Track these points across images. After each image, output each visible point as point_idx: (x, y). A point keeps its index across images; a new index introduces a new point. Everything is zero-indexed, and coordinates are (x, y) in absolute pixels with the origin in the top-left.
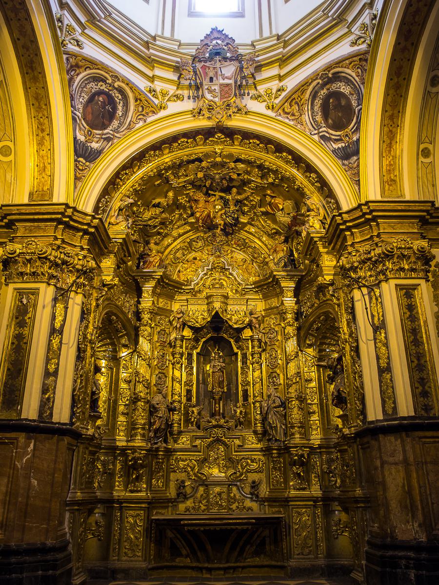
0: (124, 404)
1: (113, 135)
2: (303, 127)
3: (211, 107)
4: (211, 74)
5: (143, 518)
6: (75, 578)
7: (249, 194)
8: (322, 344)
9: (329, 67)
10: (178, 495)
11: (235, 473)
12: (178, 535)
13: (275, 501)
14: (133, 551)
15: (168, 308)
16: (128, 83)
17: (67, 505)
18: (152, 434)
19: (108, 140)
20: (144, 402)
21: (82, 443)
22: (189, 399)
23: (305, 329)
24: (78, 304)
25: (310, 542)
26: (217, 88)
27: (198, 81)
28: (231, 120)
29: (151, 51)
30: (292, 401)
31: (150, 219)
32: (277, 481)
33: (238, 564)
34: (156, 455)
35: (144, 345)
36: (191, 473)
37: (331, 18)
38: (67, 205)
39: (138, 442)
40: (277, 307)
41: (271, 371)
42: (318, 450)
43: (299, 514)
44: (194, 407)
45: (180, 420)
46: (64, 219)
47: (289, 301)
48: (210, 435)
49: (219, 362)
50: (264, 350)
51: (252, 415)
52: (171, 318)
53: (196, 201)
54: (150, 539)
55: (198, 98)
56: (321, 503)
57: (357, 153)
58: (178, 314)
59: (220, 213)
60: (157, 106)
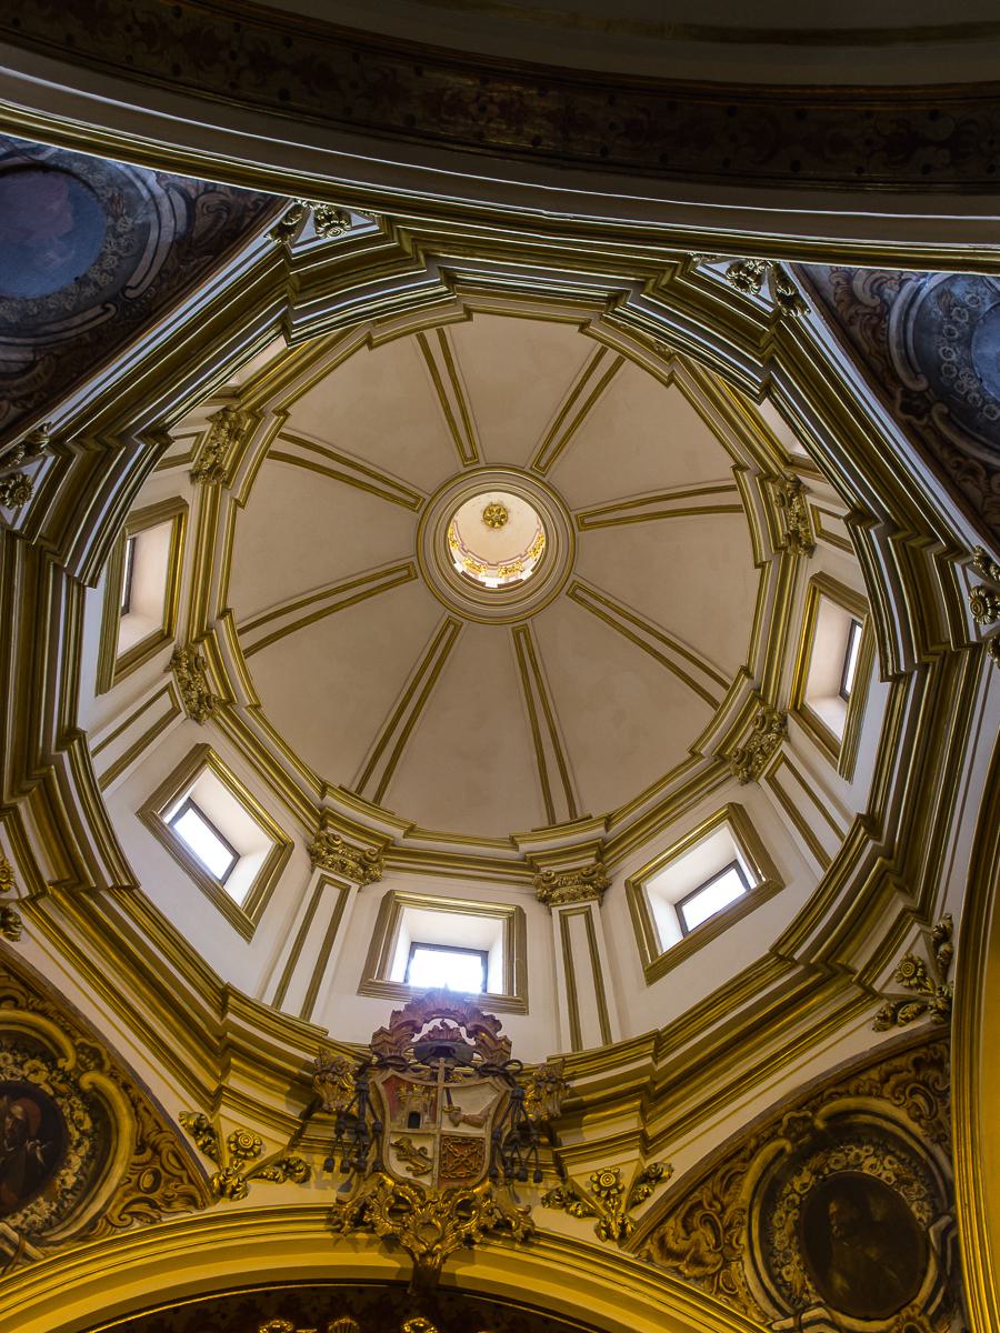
1: (16, 1247)
3: (402, 1207)
4: (415, 1104)
9: (812, 1096)
16: (130, 1083)
27: (369, 1120)
28: (471, 1261)
29: (230, 1016)
37: (801, 968)
60: (209, 1181)
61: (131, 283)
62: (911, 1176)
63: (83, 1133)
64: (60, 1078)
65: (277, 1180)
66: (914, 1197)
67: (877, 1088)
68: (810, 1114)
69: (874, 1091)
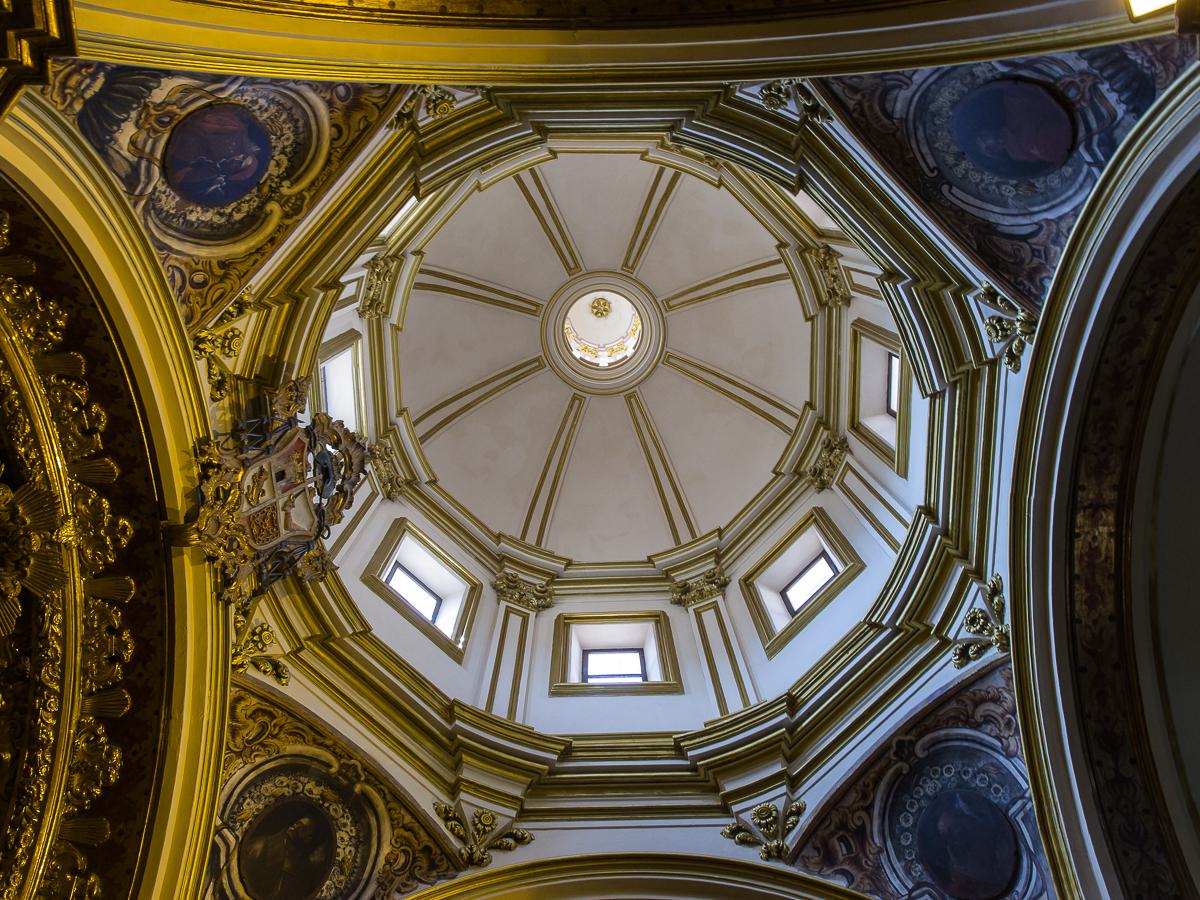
1: (141, 194)
9: (377, 777)
19: (131, 181)
37: (449, 727)
61: (955, 190)
62: (347, 872)
63: (231, 215)
64: (273, 185)
65: (209, 377)
66: (334, 880)
67: (398, 823)
68: (363, 779)
69: (396, 822)
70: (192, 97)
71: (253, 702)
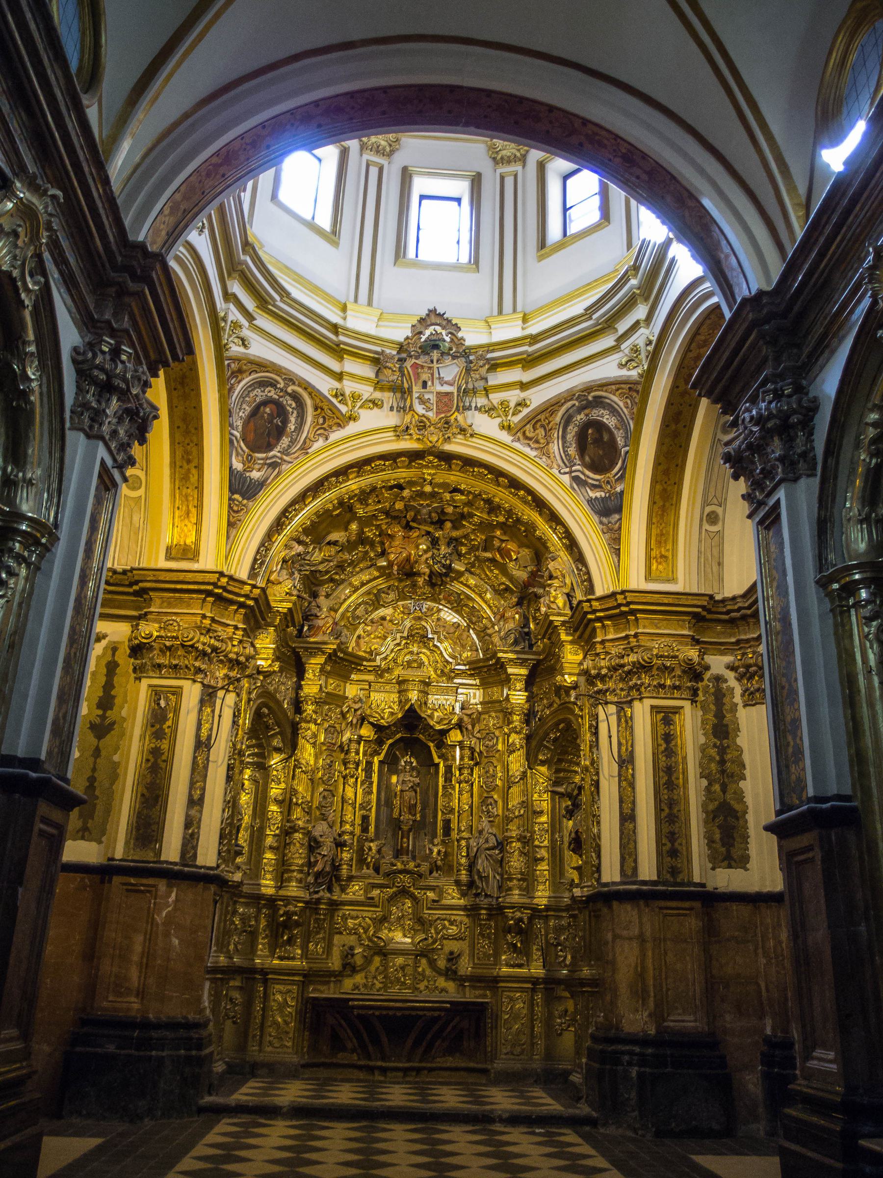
0: (272, 833)
2: (549, 461)
4: (425, 376)
5: (295, 995)
6: (216, 1065)
7: (469, 531)
8: (560, 761)
9: (589, 389)
10: (345, 966)
11: (426, 939)
12: (343, 1022)
13: (480, 981)
14: (281, 1039)
15: (341, 693)
16: (308, 387)
17: (208, 972)
18: (311, 879)
19: (274, 465)
20: (303, 834)
21: (227, 892)
22: (365, 829)
23: (538, 738)
24: (229, 707)
25: (524, 1039)
26: (433, 398)
27: (406, 385)
30: (512, 842)
31: (322, 563)
32: (484, 954)
33: (423, 1065)
34: (316, 909)
35: (307, 754)
36: (364, 936)
38: (222, 574)
39: (293, 890)
40: (501, 702)
41: (485, 795)
42: (544, 914)
43: (511, 999)
44: (372, 841)
45: (351, 860)
46: (216, 591)
47: (518, 697)
48: (394, 884)
49: (411, 776)
50: (477, 764)
51: (455, 857)
52: (345, 709)
53: (391, 537)
54: (304, 1026)
55: (404, 411)
56: (542, 986)
57: (619, 510)
58: (355, 703)
59: (425, 557)
70: (240, 451)
71: (529, 427)
